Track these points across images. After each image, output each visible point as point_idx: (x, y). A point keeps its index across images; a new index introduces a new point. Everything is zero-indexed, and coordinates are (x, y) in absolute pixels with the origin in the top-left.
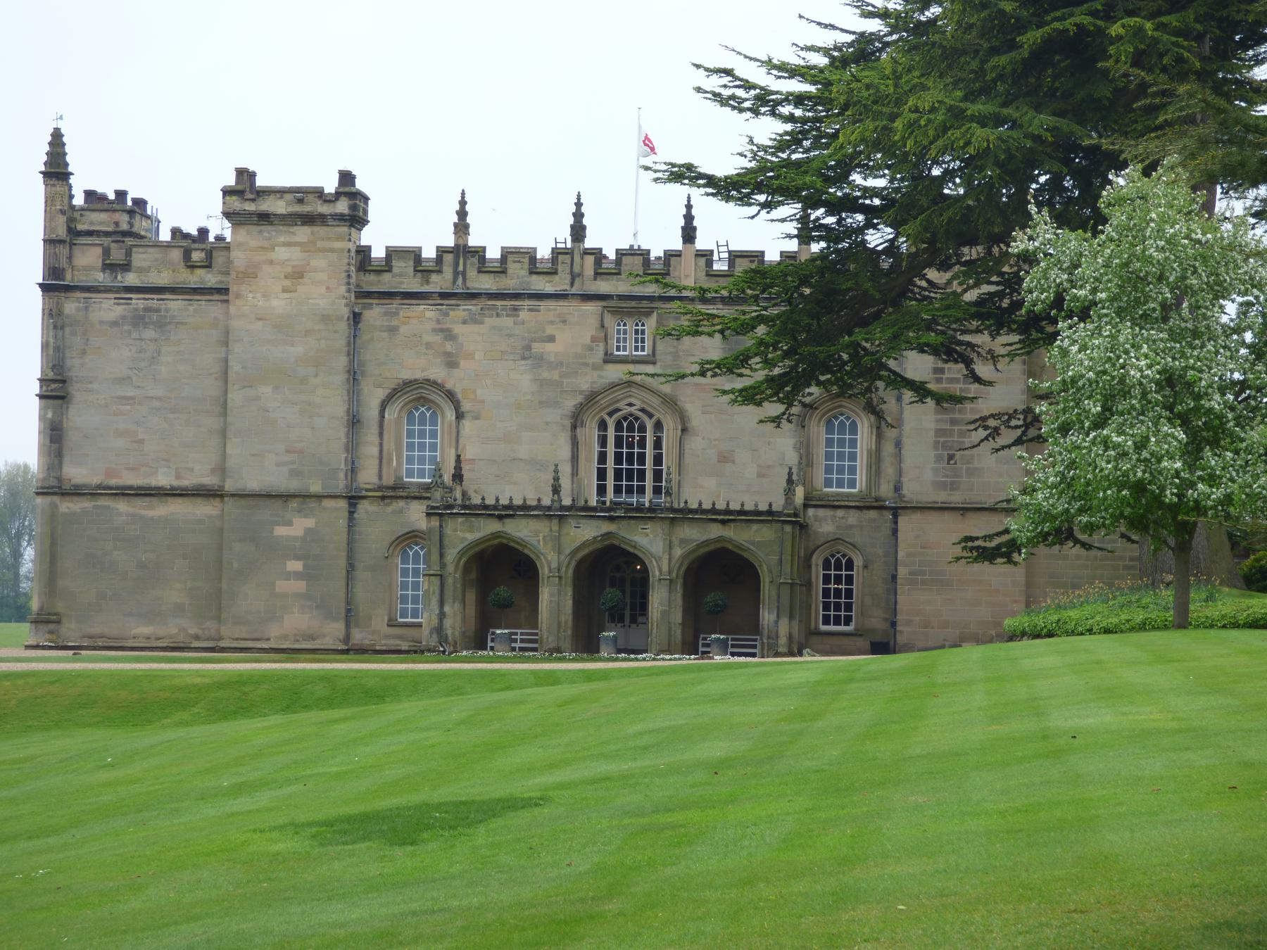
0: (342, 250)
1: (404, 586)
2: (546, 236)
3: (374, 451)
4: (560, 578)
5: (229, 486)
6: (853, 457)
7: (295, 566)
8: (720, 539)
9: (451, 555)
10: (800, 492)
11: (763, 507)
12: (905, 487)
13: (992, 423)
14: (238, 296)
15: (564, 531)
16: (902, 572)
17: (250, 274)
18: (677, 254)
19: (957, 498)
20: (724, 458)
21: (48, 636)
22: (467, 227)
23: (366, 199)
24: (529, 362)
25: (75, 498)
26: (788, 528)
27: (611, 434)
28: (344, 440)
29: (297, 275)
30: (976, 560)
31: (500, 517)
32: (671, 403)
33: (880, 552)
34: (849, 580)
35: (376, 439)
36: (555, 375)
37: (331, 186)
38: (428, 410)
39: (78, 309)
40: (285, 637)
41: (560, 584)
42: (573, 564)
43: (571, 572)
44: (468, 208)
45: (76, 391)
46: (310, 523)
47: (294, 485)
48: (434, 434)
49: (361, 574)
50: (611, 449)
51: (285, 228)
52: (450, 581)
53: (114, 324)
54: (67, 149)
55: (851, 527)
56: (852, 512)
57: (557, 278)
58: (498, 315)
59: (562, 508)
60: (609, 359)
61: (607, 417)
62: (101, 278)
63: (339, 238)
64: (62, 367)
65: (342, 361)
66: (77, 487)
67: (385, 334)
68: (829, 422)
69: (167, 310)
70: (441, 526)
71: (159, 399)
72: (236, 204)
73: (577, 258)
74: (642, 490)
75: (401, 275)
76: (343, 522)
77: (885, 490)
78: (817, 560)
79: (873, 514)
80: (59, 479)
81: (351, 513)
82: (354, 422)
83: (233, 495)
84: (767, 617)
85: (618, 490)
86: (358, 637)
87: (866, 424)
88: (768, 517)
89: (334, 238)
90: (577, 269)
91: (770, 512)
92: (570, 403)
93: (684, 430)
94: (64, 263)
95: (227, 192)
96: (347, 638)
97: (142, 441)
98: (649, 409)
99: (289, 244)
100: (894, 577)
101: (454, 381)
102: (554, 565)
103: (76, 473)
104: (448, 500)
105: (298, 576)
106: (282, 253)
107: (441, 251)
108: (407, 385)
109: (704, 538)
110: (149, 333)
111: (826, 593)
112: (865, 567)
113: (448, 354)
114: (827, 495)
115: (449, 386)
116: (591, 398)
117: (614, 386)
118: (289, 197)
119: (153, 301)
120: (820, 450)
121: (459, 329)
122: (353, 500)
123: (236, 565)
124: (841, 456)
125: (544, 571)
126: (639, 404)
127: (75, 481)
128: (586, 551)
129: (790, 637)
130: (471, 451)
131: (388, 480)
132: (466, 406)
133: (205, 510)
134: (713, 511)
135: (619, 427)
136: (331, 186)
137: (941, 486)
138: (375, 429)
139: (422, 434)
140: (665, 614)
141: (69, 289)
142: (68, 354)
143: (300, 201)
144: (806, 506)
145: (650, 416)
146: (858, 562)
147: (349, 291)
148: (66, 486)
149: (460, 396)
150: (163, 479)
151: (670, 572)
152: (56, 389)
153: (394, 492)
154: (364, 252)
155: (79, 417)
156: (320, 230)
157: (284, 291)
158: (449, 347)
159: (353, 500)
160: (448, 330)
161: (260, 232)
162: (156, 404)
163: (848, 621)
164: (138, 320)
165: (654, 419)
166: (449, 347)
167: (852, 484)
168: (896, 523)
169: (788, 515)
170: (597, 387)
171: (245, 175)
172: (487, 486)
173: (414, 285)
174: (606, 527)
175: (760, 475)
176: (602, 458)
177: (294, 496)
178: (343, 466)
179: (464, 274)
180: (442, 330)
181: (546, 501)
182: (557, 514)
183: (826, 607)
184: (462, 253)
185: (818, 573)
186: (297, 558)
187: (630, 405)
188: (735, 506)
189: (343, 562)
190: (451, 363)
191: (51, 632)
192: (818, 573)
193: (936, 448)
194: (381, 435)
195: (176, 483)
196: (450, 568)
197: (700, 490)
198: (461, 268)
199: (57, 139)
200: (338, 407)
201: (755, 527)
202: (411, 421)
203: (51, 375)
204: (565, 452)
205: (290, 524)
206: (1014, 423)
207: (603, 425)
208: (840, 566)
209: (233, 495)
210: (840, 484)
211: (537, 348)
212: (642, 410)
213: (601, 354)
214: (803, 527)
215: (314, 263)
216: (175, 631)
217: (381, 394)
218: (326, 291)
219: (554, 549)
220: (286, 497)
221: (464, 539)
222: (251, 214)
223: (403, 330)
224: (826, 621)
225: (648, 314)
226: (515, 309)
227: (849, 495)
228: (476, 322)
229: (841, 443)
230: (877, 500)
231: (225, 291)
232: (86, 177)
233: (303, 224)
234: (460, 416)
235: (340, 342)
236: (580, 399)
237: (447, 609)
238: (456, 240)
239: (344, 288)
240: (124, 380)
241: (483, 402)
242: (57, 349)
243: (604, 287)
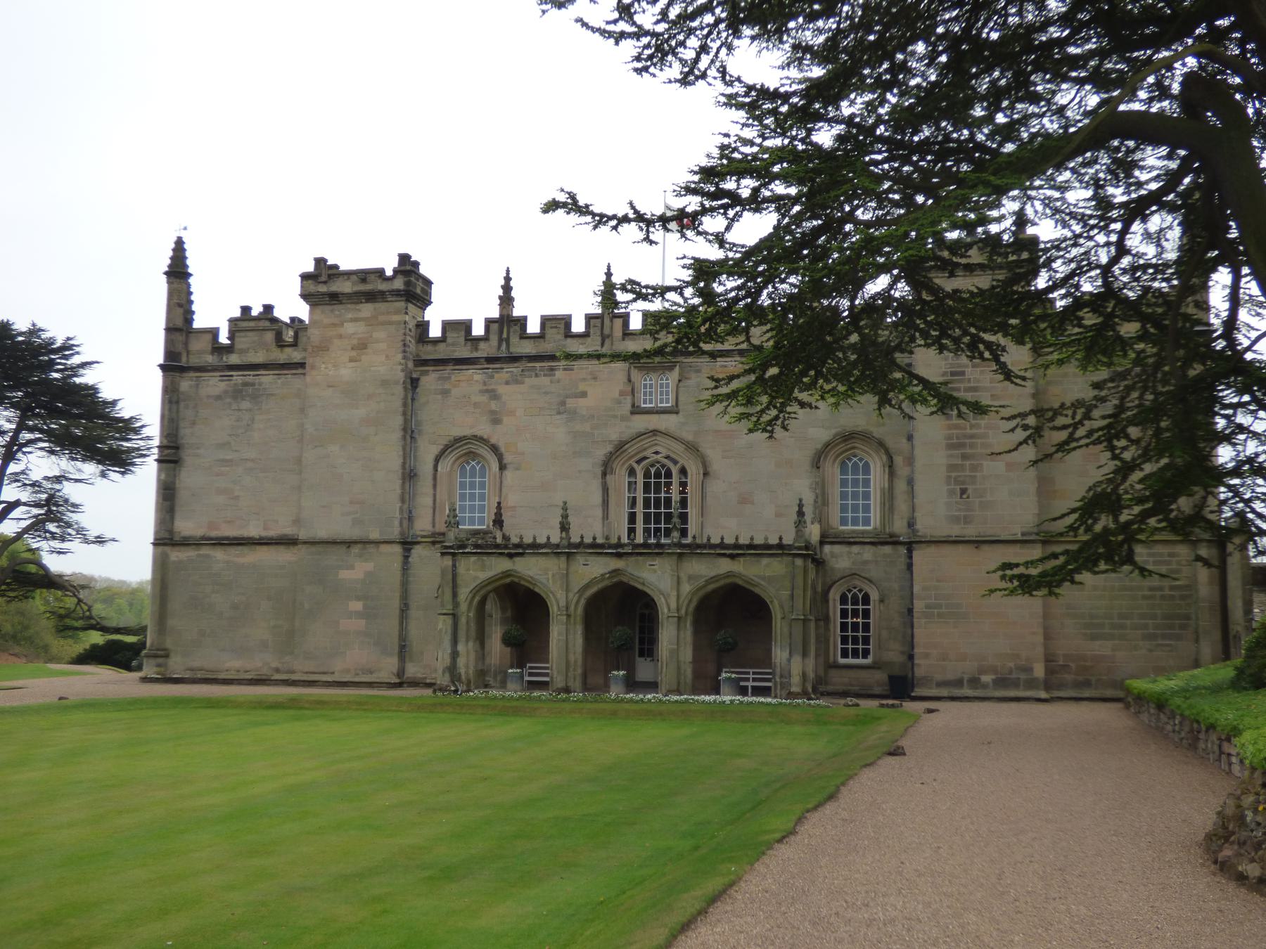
0: (399, 323)
3: (429, 501)
4: (568, 616)
5: (303, 535)
6: (867, 496)
7: (357, 606)
8: (730, 574)
9: (464, 593)
11: (774, 540)
12: (919, 522)
14: (313, 367)
15: (572, 569)
16: (918, 605)
17: (323, 348)
19: (971, 532)
20: (744, 500)
21: (155, 669)
22: (512, 299)
23: (428, 283)
24: (564, 416)
25: (182, 548)
26: (799, 562)
27: (640, 479)
28: (399, 491)
29: (362, 346)
30: (1012, 592)
31: (511, 556)
32: (692, 448)
33: (896, 586)
34: (866, 614)
36: (587, 427)
37: (390, 266)
38: (478, 463)
39: (191, 386)
40: (348, 671)
41: (567, 623)
42: (583, 602)
43: (580, 610)
44: (512, 283)
45: (188, 459)
46: (369, 566)
47: (355, 533)
48: (482, 486)
49: (414, 613)
50: (640, 495)
51: (352, 306)
52: (463, 620)
53: (218, 398)
54: (187, 254)
55: (866, 562)
56: (867, 547)
57: (589, 340)
58: (537, 375)
59: (570, 545)
60: (636, 410)
61: (635, 466)
62: (210, 359)
63: (397, 312)
64: (176, 436)
65: (398, 421)
66: (185, 538)
67: (439, 397)
68: (843, 464)
69: (260, 384)
70: (454, 566)
71: (253, 460)
72: (312, 287)
73: (607, 321)
75: (453, 345)
76: (397, 565)
77: (899, 526)
78: (834, 595)
79: (887, 549)
80: (171, 532)
81: (406, 557)
82: (410, 475)
83: (305, 543)
84: (779, 654)
86: (412, 670)
87: (879, 464)
88: (780, 549)
89: (394, 311)
90: (607, 331)
91: (780, 546)
92: (601, 452)
93: (706, 474)
94: (179, 347)
95: (305, 277)
96: (401, 673)
97: (237, 498)
98: (672, 455)
99: (352, 320)
100: (910, 611)
101: (497, 436)
102: (563, 603)
103: (185, 526)
105: (359, 615)
107: (489, 322)
108: (458, 440)
109: (713, 574)
110: (246, 405)
111: (844, 627)
112: (882, 601)
113: (493, 412)
114: (843, 532)
115: (493, 441)
116: (620, 447)
118: (354, 277)
119: (250, 376)
120: (835, 491)
121: (502, 389)
122: (407, 544)
123: (307, 606)
124: (855, 496)
125: (554, 609)
126: (664, 452)
127: (186, 533)
129: (804, 675)
130: (512, 499)
132: (508, 458)
135: (647, 475)
137: (956, 520)
138: (429, 482)
139: (472, 486)
140: (675, 653)
141: (183, 369)
142: (182, 424)
143: (364, 281)
144: (822, 543)
145: (675, 462)
146: (874, 596)
147: (404, 358)
148: (177, 538)
149: (503, 450)
150: (254, 531)
151: (678, 610)
154: (424, 326)
155: (189, 478)
156: (381, 306)
157: (351, 361)
158: (494, 405)
159: (407, 544)
160: (493, 391)
161: (332, 311)
162: (250, 464)
163: (866, 654)
164: (237, 394)
165: (678, 466)
166: (494, 405)
167: (867, 521)
168: (911, 557)
169: (799, 548)
170: (625, 437)
173: (465, 352)
175: (778, 515)
176: (633, 502)
177: (356, 542)
178: (397, 514)
179: (508, 340)
180: (487, 391)
181: (555, 539)
182: (568, 550)
183: (844, 640)
185: (835, 608)
186: (358, 599)
187: (657, 453)
188: (744, 540)
189: (396, 603)
190: (496, 421)
191: (159, 665)
192: (835, 608)
193: (948, 483)
194: (435, 486)
195: (264, 534)
196: (463, 607)
198: (505, 335)
199: (179, 247)
200: (394, 461)
201: (765, 561)
202: (463, 475)
203: (165, 442)
204: (597, 498)
205: (352, 567)
206: (1061, 421)
207: (632, 472)
208: (857, 603)
209: (305, 543)
210: (855, 521)
211: (571, 403)
212: (667, 457)
213: (628, 407)
214: (819, 563)
215: (375, 335)
216: (260, 664)
217: (435, 450)
218: (386, 361)
219: (563, 586)
220: (349, 544)
221: (476, 578)
222: (323, 294)
223: (455, 392)
224: (845, 654)
225: (671, 368)
226: (552, 369)
227: (863, 532)
228: (517, 382)
229: (855, 483)
230: (891, 536)
231: (302, 365)
233: (368, 301)
234: (502, 467)
235: (397, 404)
236: (610, 448)
237: (461, 648)
238: (501, 310)
239: (400, 356)
240: (222, 446)
241: (523, 454)
242: (171, 420)
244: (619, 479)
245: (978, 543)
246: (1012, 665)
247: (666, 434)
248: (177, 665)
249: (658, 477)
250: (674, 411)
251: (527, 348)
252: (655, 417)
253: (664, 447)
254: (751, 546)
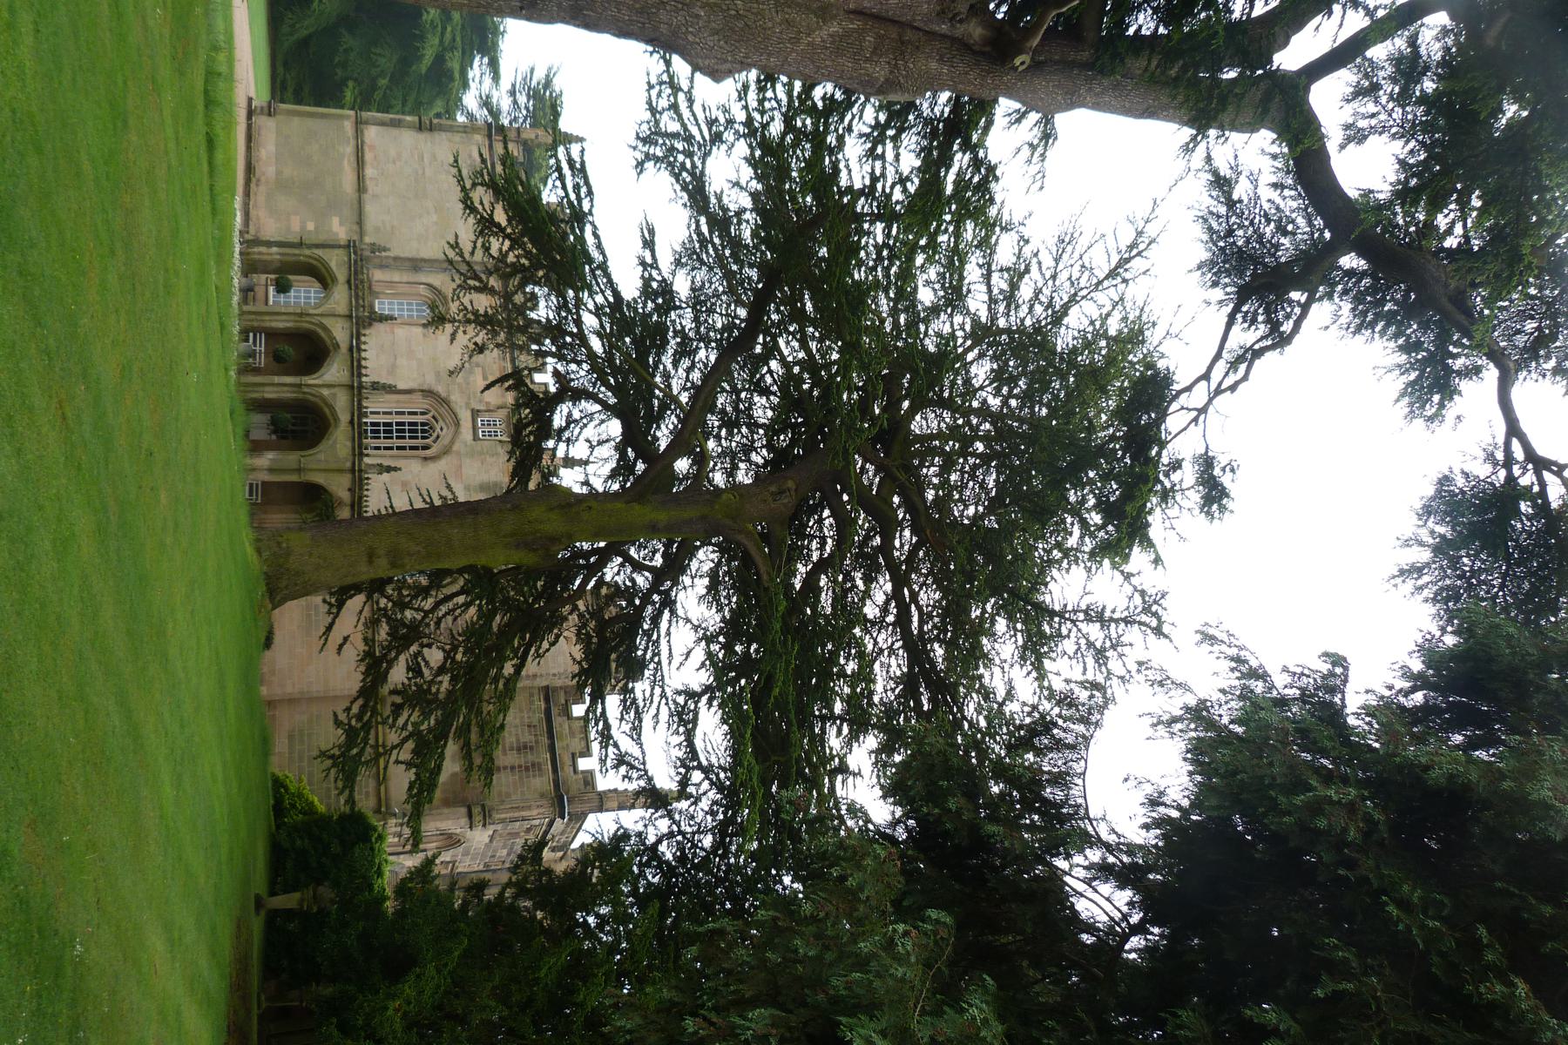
4: (301, 315)
5: (366, 197)
8: (336, 419)
9: (319, 252)
31: (349, 282)
35: (405, 279)
45: (422, 136)
52: (296, 251)
60: (475, 413)
82: (416, 264)
92: (440, 389)
93: (425, 459)
116: (444, 401)
128: (323, 334)
130: (401, 332)
135: (423, 424)
141: (490, 136)
150: (369, 172)
172: (376, 345)
196: (307, 252)
201: (349, 444)
205: (341, 224)
220: (360, 223)
236: (443, 395)
237: (275, 249)
244: (420, 403)
246: (265, 670)
247: (457, 432)
248: (260, 121)
252: (470, 425)
253: (446, 435)
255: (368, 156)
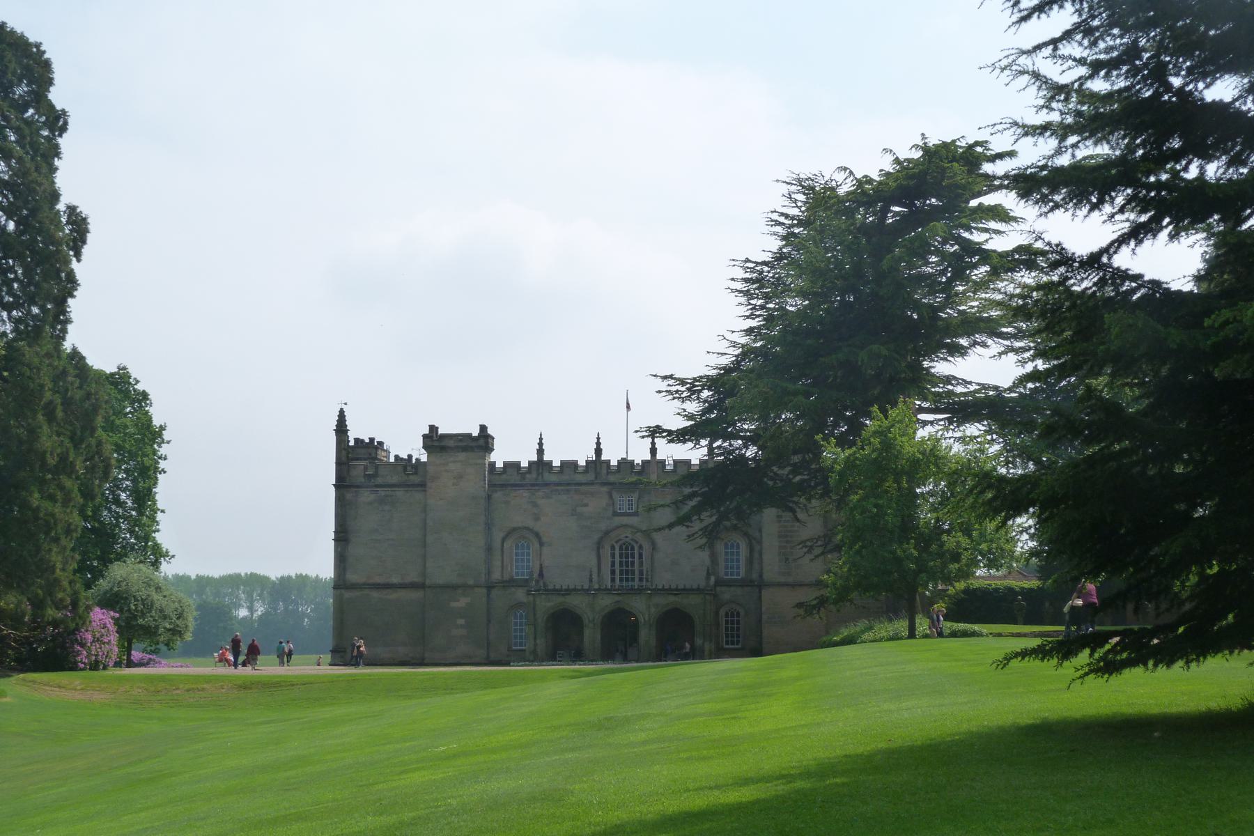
1: (516, 631)
2: (583, 455)
3: (499, 563)
6: (738, 561)
7: (461, 622)
10: (713, 579)
11: (695, 586)
13: (809, 544)
16: (764, 617)
18: (647, 462)
19: (790, 580)
27: (617, 552)
29: (460, 477)
34: (738, 622)
37: (476, 433)
46: (468, 600)
48: (528, 554)
50: (617, 560)
53: (370, 503)
60: (615, 514)
74: (633, 580)
76: (484, 599)
77: (755, 576)
78: (722, 612)
81: (488, 595)
82: (489, 549)
85: (621, 580)
88: (698, 591)
91: (698, 589)
92: (596, 537)
95: (425, 436)
100: (760, 621)
103: (352, 577)
104: (539, 585)
106: (452, 466)
108: (514, 529)
110: (387, 508)
111: (727, 629)
116: (607, 533)
117: (618, 527)
124: (732, 560)
125: (586, 621)
131: (506, 577)
132: (544, 539)
133: (415, 595)
134: (670, 589)
135: (621, 548)
136: (476, 433)
139: (523, 554)
146: (742, 613)
150: (395, 580)
152: (342, 536)
153: (510, 583)
154: (493, 465)
159: (490, 587)
163: (738, 642)
167: (738, 574)
171: (433, 429)
172: (556, 580)
174: (617, 598)
176: (613, 564)
181: (586, 587)
183: (727, 636)
184: (540, 465)
188: (681, 587)
197: (664, 579)
199: (342, 413)
202: (517, 548)
204: (594, 561)
207: (613, 548)
214: (715, 596)
217: (502, 535)
219: (592, 610)
220: (454, 587)
224: (727, 643)
229: (732, 554)
232: (355, 432)
234: (541, 544)
243: (612, 478)
244: (606, 551)
245: (793, 586)
249: (627, 550)
250: (636, 514)
251: (554, 478)
254: (684, 590)
255: (378, 580)
